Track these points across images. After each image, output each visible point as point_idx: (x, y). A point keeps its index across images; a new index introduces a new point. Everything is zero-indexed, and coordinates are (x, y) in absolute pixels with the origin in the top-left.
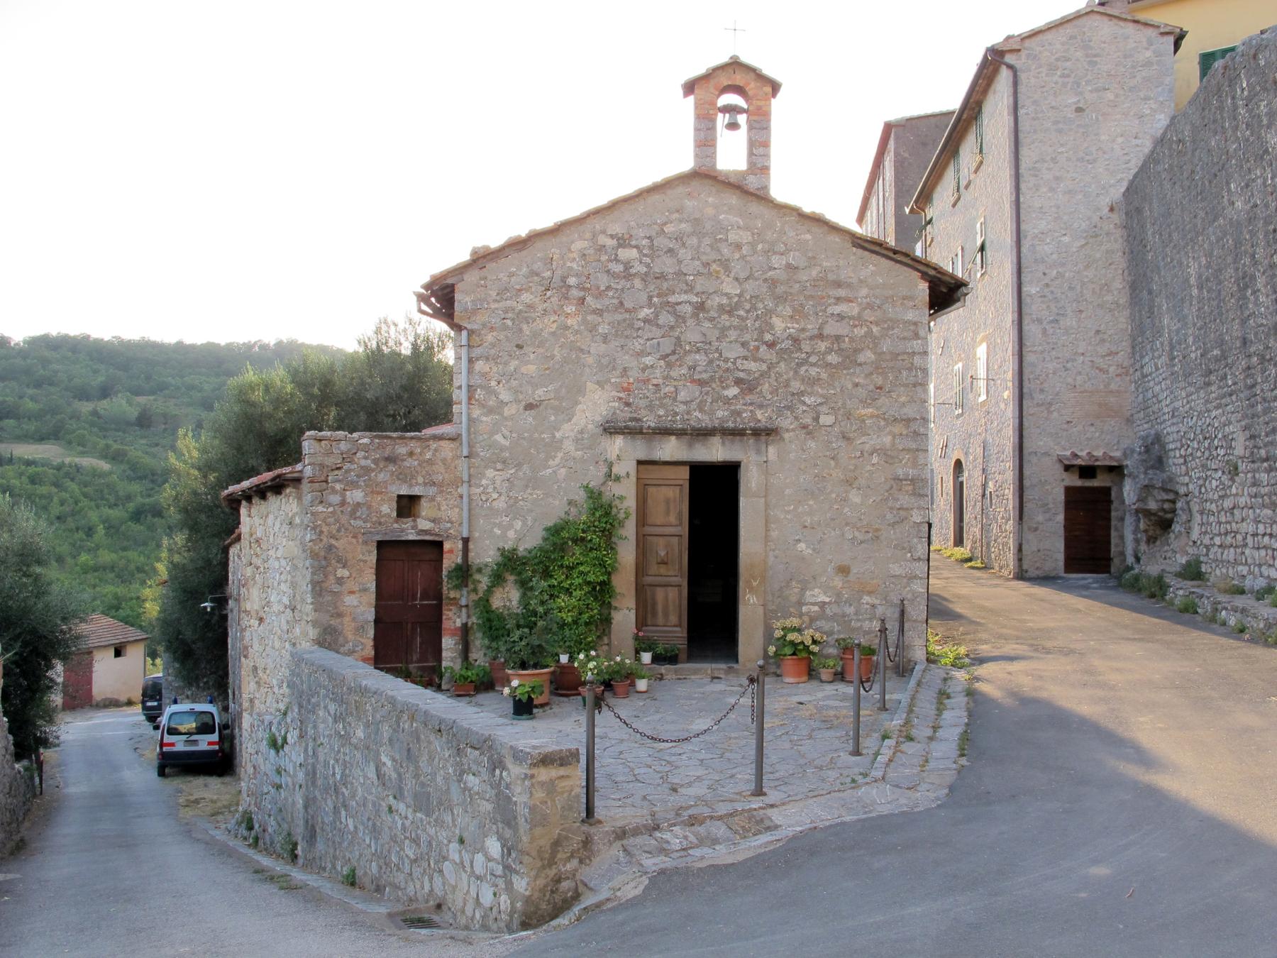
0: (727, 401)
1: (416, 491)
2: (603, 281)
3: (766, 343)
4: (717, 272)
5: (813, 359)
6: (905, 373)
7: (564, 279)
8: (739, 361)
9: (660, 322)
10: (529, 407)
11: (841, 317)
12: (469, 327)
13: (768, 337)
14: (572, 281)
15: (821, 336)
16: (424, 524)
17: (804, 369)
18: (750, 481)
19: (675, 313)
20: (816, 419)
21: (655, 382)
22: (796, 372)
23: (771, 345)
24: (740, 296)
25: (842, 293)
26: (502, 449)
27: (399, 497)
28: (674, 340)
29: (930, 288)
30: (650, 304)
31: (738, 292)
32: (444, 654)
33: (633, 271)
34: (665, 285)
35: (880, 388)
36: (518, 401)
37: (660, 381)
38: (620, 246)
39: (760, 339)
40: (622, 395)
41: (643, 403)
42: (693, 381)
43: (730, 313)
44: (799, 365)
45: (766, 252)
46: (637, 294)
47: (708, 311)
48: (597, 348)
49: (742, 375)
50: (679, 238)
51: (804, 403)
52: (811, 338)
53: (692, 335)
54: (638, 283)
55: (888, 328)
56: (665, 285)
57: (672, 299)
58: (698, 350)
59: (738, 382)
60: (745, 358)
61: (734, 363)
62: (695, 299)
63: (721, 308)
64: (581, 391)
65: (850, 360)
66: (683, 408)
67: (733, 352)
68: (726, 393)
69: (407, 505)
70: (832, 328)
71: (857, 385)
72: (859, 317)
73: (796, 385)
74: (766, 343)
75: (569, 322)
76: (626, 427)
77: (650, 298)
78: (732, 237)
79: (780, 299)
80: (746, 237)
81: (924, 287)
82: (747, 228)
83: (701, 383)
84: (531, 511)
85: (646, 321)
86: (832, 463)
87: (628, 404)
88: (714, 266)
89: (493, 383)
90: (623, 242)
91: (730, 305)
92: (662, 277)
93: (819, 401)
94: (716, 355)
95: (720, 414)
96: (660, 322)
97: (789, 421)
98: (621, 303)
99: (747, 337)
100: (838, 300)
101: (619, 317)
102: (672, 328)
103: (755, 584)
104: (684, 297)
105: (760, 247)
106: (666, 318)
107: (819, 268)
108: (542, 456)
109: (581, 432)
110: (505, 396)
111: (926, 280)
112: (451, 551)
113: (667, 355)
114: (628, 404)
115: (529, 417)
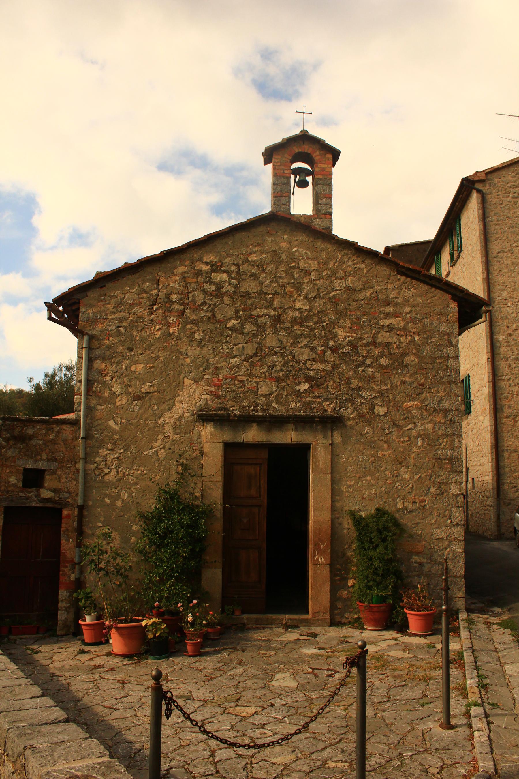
0: (299, 394)
1: (41, 465)
2: (200, 298)
3: (330, 348)
4: (291, 292)
5: (368, 362)
6: (441, 373)
7: (168, 296)
8: (309, 363)
9: (245, 331)
10: (137, 398)
11: (390, 329)
12: (90, 333)
13: (332, 343)
14: (174, 297)
15: (374, 343)
16: (46, 494)
17: (361, 369)
18: (319, 458)
19: (256, 324)
20: (372, 410)
21: (240, 378)
22: (355, 372)
23: (334, 350)
24: (310, 310)
25: (390, 309)
26: (114, 432)
27: (25, 470)
28: (255, 345)
29: (459, 306)
30: (238, 317)
31: (308, 307)
32: (60, 605)
33: (223, 290)
34: (249, 302)
35: (422, 385)
36: (128, 393)
37: (245, 378)
38: (213, 271)
39: (327, 346)
40: (212, 389)
41: (230, 396)
42: (271, 378)
43: (301, 324)
44: (358, 366)
45: (329, 277)
46: (226, 309)
47: (284, 323)
48: (194, 351)
49: (312, 374)
50: (261, 265)
51: (361, 397)
52: (367, 344)
53: (270, 341)
54: (227, 299)
55: (427, 338)
56: (249, 302)
57: (254, 313)
58: (276, 353)
59: (309, 379)
60: (314, 360)
61: (305, 364)
62: (273, 313)
63: (294, 321)
64: (180, 385)
65: (398, 362)
66: (263, 399)
67: (305, 355)
68: (298, 388)
69: (33, 479)
70: (383, 337)
71: (403, 382)
72: (404, 329)
73: (355, 383)
74: (330, 348)
75: (171, 330)
76: (216, 415)
77: (237, 312)
78: (302, 264)
79: (341, 314)
80: (313, 265)
81: (453, 306)
82: (315, 259)
83: (278, 380)
84: (136, 484)
85: (233, 329)
86: (386, 446)
87: (218, 397)
88: (289, 288)
89: (108, 378)
90: (215, 268)
91: (301, 318)
92: (246, 295)
93: (374, 395)
94: (290, 358)
95: (293, 405)
96: (245, 331)
97: (349, 411)
98: (214, 316)
99: (316, 343)
100: (388, 315)
101: (211, 326)
102: (254, 335)
103: (323, 546)
104: (265, 311)
105: (324, 273)
106: (249, 328)
107: (372, 290)
108: (146, 438)
109: (180, 419)
110: (117, 389)
111: (455, 301)
112: (68, 516)
113: (251, 357)
114: (218, 397)
115: (136, 407)
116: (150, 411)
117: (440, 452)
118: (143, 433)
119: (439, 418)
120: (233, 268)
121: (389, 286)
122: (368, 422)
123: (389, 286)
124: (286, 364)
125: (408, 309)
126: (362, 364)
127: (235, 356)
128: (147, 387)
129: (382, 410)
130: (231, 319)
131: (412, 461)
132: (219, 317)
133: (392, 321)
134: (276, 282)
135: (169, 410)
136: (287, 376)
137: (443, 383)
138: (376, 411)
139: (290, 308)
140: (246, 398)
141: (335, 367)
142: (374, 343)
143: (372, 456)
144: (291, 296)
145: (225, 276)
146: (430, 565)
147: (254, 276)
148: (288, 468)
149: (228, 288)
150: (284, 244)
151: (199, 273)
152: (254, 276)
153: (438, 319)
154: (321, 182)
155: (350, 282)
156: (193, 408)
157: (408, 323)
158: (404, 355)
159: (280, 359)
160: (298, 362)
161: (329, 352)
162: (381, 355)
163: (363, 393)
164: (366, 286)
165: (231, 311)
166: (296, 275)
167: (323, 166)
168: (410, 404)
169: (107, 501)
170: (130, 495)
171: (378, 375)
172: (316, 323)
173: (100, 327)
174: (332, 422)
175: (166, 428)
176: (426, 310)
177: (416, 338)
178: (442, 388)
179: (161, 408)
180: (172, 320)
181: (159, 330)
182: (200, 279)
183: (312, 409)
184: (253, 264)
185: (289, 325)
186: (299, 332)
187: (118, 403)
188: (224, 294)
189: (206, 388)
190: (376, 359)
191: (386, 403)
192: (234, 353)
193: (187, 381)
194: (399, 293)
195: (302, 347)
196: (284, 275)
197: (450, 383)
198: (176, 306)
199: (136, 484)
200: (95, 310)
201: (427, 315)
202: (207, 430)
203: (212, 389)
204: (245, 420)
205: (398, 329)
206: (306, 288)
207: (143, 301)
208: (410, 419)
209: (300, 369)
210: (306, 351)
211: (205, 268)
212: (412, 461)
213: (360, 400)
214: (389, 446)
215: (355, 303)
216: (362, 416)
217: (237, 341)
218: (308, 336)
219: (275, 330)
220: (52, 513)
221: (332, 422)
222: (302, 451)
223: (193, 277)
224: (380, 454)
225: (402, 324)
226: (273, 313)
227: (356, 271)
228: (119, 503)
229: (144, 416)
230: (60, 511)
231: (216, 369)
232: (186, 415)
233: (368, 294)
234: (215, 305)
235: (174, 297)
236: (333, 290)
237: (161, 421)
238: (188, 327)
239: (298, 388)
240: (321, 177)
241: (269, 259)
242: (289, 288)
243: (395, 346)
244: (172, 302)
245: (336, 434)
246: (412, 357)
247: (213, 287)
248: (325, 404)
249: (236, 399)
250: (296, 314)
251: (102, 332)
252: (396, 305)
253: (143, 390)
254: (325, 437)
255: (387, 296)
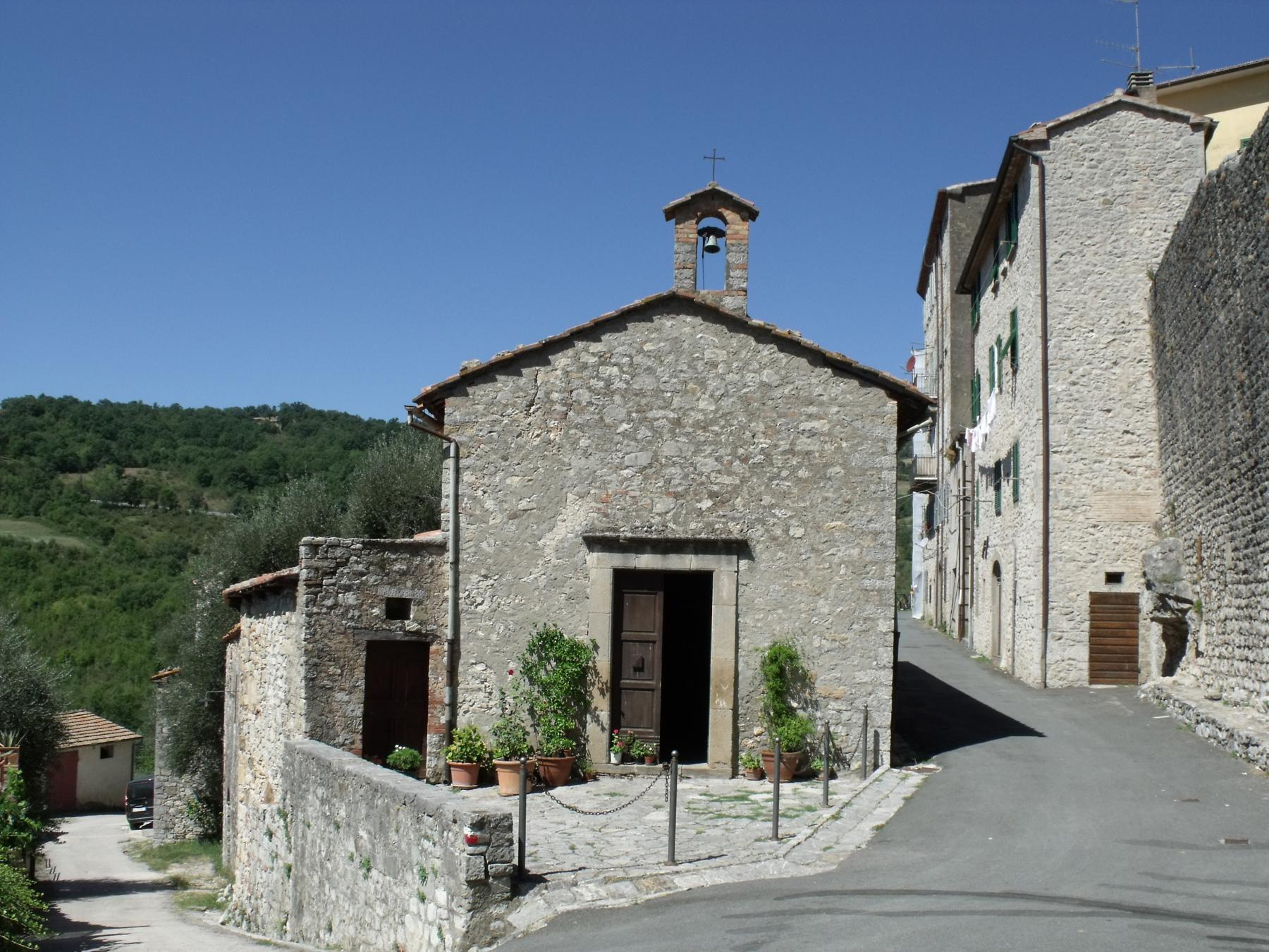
0: (700, 513)
1: (406, 594)
2: (585, 396)
3: (739, 458)
4: (694, 390)
5: (784, 473)
6: (873, 487)
7: (548, 394)
8: (713, 475)
9: (639, 437)
10: (514, 516)
11: (812, 434)
12: (457, 439)
13: (741, 451)
14: (555, 396)
15: (791, 452)
16: (411, 625)
17: (775, 482)
18: (722, 589)
19: (652, 428)
20: (786, 531)
21: (632, 494)
22: (767, 486)
23: (744, 460)
24: (716, 411)
25: (812, 409)
26: (488, 556)
27: (388, 599)
28: (650, 454)
29: (898, 405)
30: (629, 421)
31: (713, 408)
32: (428, 749)
33: (613, 387)
34: (644, 401)
35: (849, 502)
36: (502, 511)
37: (638, 493)
38: (602, 364)
39: (735, 455)
40: (599, 506)
41: (620, 515)
42: (668, 494)
43: (705, 429)
44: (771, 479)
45: (740, 369)
46: (616, 410)
47: (684, 427)
48: (578, 462)
49: (716, 488)
50: (658, 356)
51: (774, 516)
52: (784, 453)
53: (668, 448)
54: (617, 398)
55: (857, 445)
56: (644, 401)
57: (650, 415)
58: (674, 464)
59: (712, 495)
60: (719, 472)
61: (708, 477)
62: (672, 415)
63: (697, 424)
64: (562, 502)
65: (820, 474)
66: (658, 519)
67: (707, 464)
68: (699, 505)
69: (397, 609)
70: (804, 443)
71: (826, 499)
72: (829, 434)
73: (767, 500)
74: (739, 458)
75: (552, 436)
76: (604, 538)
77: (629, 413)
78: (708, 355)
79: (752, 416)
80: (722, 355)
81: (892, 405)
82: (723, 348)
83: (677, 496)
84: (513, 615)
85: (624, 434)
86: (801, 574)
87: (606, 515)
88: (691, 385)
89: (480, 493)
90: (604, 359)
91: (705, 421)
92: (640, 393)
93: (790, 513)
94: (691, 469)
95: (693, 526)
96: (639, 437)
97: (759, 533)
98: (602, 418)
99: (722, 452)
100: (810, 417)
101: (598, 432)
102: (649, 442)
103: (725, 689)
104: (661, 413)
105: (735, 365)
106: (643, 432)
107: (791, 387)
108: (524, 563)
109: (562, 541)
110: (490, 504)
111: (895, 399)
112: (437, 651)
113: (645, 468)
114: (606, 515)
115: (512, 526)
116: (529, 531)
117: (867, 582)
118: (520, 556)
119: (867, 542)
120: (626, 360)
121: (814, 381)
122: (781, 546)
123: (814, 381)
124: (686, 476)
125: (835, 409)
126: (777, 476)
127: (627, 467)
128: (523, 504)
129: (799, 532)
130: (623, 421)
131: (832, 593)
132: (608, 420)
133: (815, 424)
134: (676, 377)
135: (551, 530)
136: (687, 491)
137: (874, 500)
138: (791, 533)
139: (692, 409)
140: (638, 517)
141: (743, 481)
142: (791, 452)
143: (786, 585)
144: (694, 394)
145: (615, 369)
146: (849, 713)
147: (650, 370)
148: (686, 603)
149: (618, 384)
150: (687, 330)
151: (585, 366)
152: (650, 370)
153: (872, 421)
154: (733, 248)
155: (767, 375)
156: (578, 528)
157: (834, 426)
158: (827, 466)
159: (679, 471)
160: (701, 474)
161: (738, 462)
162: (800, 466)
163: (776, 511)
164: (785, 381)
165: (622, 413)
166: (700, 368)
167: (737, 227)
168: (834, 524)
169: (480, 634)
170: (507, 628)
171: (795, 491)
172: (723, 427)
173: (470, 432)
174: (739, 548)
175: (548, 551)
176: (858, 410)
177: (844, 445)
178: (872, 506)
179: (542, 527)
180: (552, 424)
181: (538, 436)
182: (586, 373)
183: (714, 531)
184: (647, 355)
185: (691, 430)
186: (703, 439)
187: (491, 522)
188: (613, 392)
189: (593, 504)
190: (794, 470)
191: (804, 524)
192: (626, 464)
193: (571, 497)
194: (825, 390)
195: (705, 457)
196: (685, 368)
197: (883, 500)
198: (558, 407)
199: (513, 615)
200: (463, 410)
201: (860, 416)
202: (593, 558)
203: (599, 506)
204: (637, 545)
205: (822, 434)
206: (712, 384)
207: (519, 401)
208: (831, 542)
209: (702, 483)
210: (711, 461)
211: (593, 360)
212: (832, 593)
213: (772, 520)
214: (806, 574)
215: (770, 402)
216: (774, 539)
217: (629, 449)
218: (715, 443)
219: (674, 435)
220: (419, 648)
221: (739, 548)
222: (704, 580)
223: (578, 372)
224: (795, 583)
225: (826, 428)
226: (672, 415)
227: (773, 362)
228: (494, 637)
229: (523, 537)
230: (428, 645)
231: (604, 482)
232: (570, 535)
233: (786, 391)
234: (604, 407)
235: (555, 396)
236: (745, 386)
237: (540, 543)
238: (572, 431)
239: (699, 505)
240: (733, 242)
241: (668, 348)
242: (691, 385)
243: (817, 455)
244: (553, 402)
245: (742, 562)
246: (838, 469)
247: (602, 384)
248: (731, 525)
249: (627, 518)
250: (700, 417)
251: (471, 438)
252: (822, 404)
253: (520, 507)
254: (730, 563)
255: (811, 393)
